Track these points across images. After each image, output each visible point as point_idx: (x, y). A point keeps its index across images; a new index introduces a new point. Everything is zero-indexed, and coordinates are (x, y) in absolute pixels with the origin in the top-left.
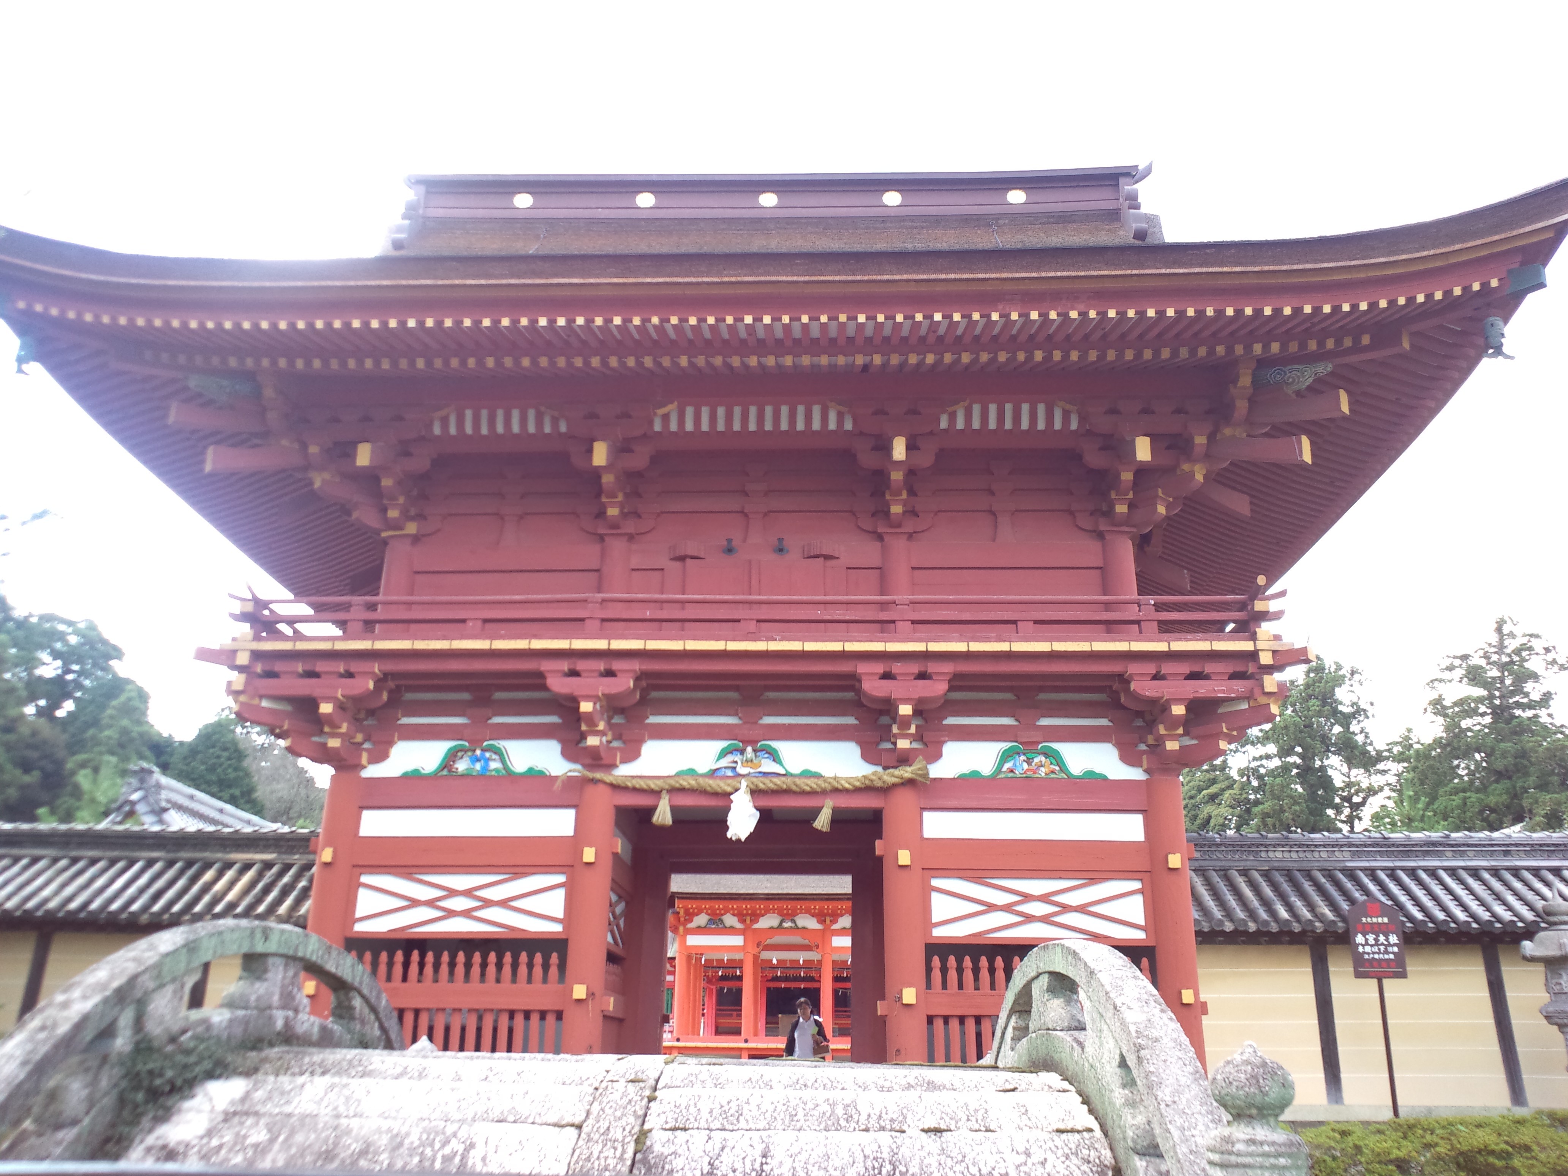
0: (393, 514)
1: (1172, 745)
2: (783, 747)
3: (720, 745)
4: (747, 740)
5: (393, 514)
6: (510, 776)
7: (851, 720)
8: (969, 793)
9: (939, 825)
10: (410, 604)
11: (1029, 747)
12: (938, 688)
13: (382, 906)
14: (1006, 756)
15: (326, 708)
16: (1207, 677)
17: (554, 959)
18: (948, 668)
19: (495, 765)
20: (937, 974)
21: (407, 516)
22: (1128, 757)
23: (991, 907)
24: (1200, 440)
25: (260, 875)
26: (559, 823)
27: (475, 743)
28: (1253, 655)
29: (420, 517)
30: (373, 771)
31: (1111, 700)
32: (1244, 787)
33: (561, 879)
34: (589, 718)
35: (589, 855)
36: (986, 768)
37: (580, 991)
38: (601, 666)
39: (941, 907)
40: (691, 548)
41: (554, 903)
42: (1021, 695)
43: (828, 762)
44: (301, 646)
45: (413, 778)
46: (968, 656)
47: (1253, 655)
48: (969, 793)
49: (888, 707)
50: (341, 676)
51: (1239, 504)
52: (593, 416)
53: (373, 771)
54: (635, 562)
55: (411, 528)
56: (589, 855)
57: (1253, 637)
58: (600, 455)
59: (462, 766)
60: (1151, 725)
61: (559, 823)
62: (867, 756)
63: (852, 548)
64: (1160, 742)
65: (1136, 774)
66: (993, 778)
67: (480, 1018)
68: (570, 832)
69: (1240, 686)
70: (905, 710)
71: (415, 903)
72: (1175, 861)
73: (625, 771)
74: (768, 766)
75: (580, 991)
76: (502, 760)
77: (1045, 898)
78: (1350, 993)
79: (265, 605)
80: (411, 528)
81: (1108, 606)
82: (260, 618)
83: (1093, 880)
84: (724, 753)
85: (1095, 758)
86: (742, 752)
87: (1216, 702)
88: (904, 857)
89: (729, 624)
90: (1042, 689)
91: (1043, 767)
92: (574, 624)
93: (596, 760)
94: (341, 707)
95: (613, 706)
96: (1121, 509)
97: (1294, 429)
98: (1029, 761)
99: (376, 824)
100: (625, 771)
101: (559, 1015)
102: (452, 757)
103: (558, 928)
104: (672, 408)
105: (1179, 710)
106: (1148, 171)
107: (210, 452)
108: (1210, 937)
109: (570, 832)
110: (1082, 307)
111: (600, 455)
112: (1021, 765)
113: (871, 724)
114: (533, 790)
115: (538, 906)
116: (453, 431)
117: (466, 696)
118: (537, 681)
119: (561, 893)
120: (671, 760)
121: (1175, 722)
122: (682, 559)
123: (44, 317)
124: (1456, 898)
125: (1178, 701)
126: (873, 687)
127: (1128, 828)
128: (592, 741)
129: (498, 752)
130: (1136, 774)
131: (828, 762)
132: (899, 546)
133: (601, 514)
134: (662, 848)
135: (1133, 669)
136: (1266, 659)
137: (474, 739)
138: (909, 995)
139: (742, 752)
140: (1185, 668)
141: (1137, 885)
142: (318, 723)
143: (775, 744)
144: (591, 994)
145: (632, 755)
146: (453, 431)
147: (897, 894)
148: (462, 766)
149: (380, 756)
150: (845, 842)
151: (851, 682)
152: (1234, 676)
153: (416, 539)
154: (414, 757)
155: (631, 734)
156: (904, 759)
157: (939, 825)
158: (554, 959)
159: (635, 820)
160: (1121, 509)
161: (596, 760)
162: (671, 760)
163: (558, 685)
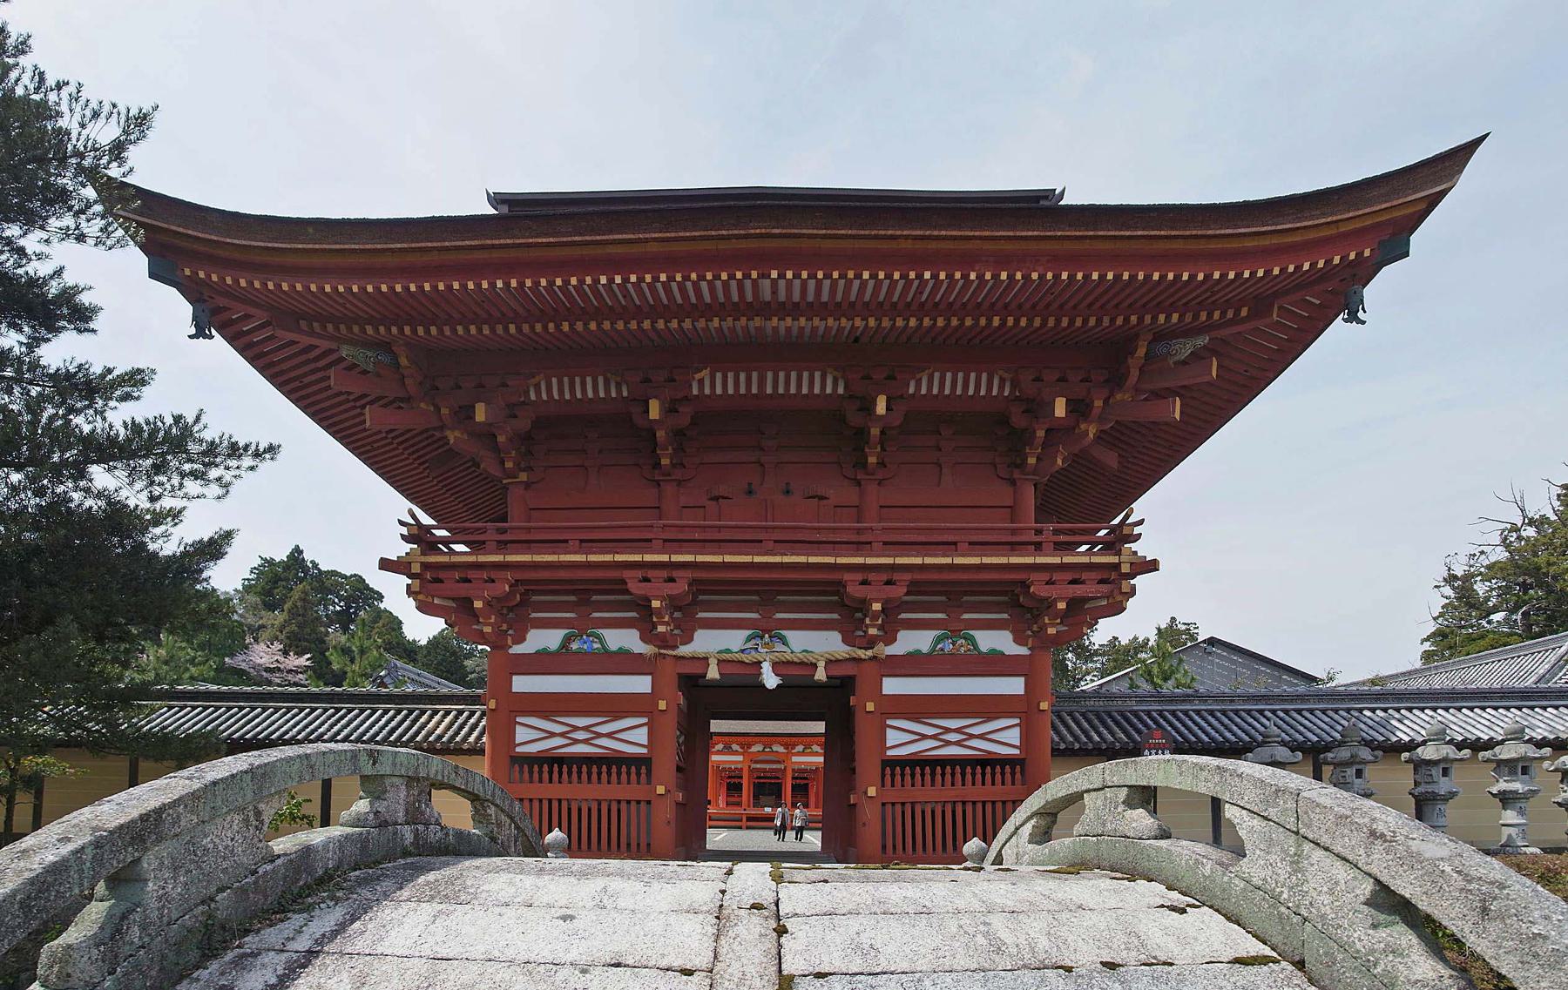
2: (790, 635)
6: (607, 653)
9: (893, 686)
10: (529, 529)
11: (955, 633)
14: (939, 640)
16: (1083, 582)
17: (643, 770)
20: (888, 778)
22: (1019, 640)
23: (924, 737)
25: (456, 718)
26: (641, 684)
29: (529, 469)
31: (1015, 601)
33: (645, 720)
34: (659, 612)
35: (662, 705)
36: (925, 649)
37: (661, 790)
38: (665, 574)
40: (722, 490)
41: (641, 736)
42: (953, 596)
43: (819, 646)
44: (455, 559)
45: (542, 654)
51: (1111, 459)
52: (647, 380)
53: (517, 649)
55: (523, 477)
56: (662, 705)
57: (1119, 553)
58: (654, 410)
59: (575, 646)
60: (1037, 617)
61: (641, 684)
63: (839, 492)
65: (1023, 651)
66: (929, 655)
70: (877, 606)
71: (552, 735)
72: (1044, 706)
73: (684, 650)
74: (779, 647)
75: (661, 790)
77: (958, 731)
80: (523, 477)
81: (1014, 531)
83: (989, 719)
84: (749, 639)
85: (997, 641)
88: (870, 707)
89: (754, 544)
90: (966, 593)
91: (963, 646)
92: (644, 544)
94: (488, 604)
95: (674, 604)
96: (1032, 461)
99: (521, 684)
100: (684, 650)
101: (649, 802)
102: (567, 640)
103: (645, 751)
104: (705, 373)
108: (1056, 752)
111: (654, 410)
112: (948, 646)
114: (623, 663)
115: (633, 737)
117: (573, 598)
118: (620, 586)
119: (645, 730)
122: (716, 499)
123: (207, 283)
124: (1201, 728)
125: (1062, 599)
127: (1014, 686)
128: (661, 629)
129: (598, 637)
130: (1023, 651)
131: (819, 646)
133: (657, 465)
134: (705, 699)
137: (581, 628)
138: (872, 791)
139: (762, 638)
140: (1069, 576)
142: (474, 615)
143: (784, 632)
144: (667, 791)
145: (689, 639)
147: (862, 727)
148: (575, 646)
149: (521, 639)
150: (831, 700)
151: (838, 587)
153: (527, 485)
156: (870, 643)
157: (893, 686)
158: (643, 770)
159: (692, 683)
160: (1032, 461)
161: (664, 642)
162: (715, 644)
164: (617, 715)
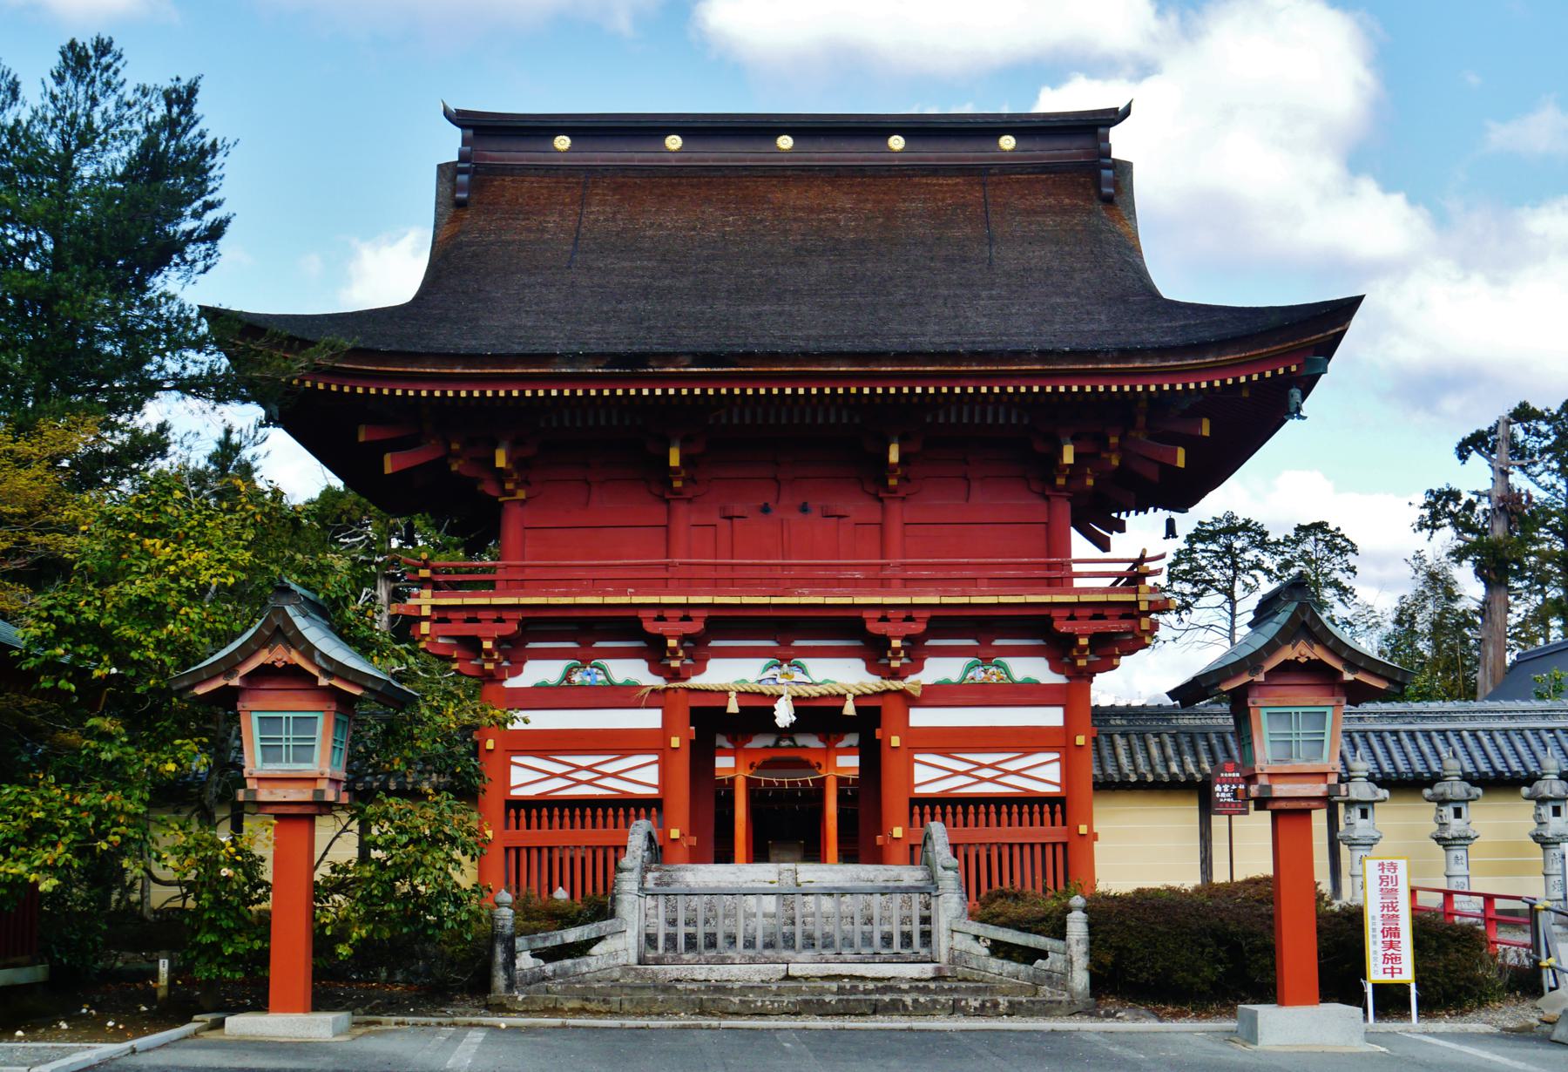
0: (509, 486)
1: (1082, 663)
4: (784, 657)
5: (509, 486)
6: (613, 687)
9: (920, 718)
11: (987, 660)
13: (528, 778)
14: (970, 668)
15: (488, 645)
18: (927, 614)
19: (601, 678)
21: (518, 486)
22: (1055, 668)
24: (1114, 440)
26: (651, 719)
27: (586, 661)
28: (1136, 603)
30: (511, 683)
32: (1470, 506)
33: (655, 758)
39: (921, 773)
41: (651, 775)
43: (842, 676)
46: (941, 605)
47: (1136, 603)
48: (939, 695)
49: (885, 641)
50: (496, 621)
54: (694, 519)
55: (521, 495)
61: (651, 719)
62: (872, 668)
63: (858, 508)
64: (1074, 660)
65: (1060, 679)
67: (594, 853)
68: (659, 725)
69: (1125, 625)
71: (553, 775)
72: (1080, 740)
73: (696, 681)
74: (799, 676)
75: (675, 834)
76: (606, 674)
78: (1219, 823)
80: (521, 495)
84: (767, 668)
86: (780, 666)
88: (895, 741)
97: (1178, 440)
98: (986, 671)
100: (696, 681)
103: (655, 791)
105: (1083, 641)
106: (1127, 112)
107: (387, 458)
109: (659, 725)
110: (1016, 383)
112: (979, 675)
113: (874, 652)
115: (641, 776)
119: (655, 768)
120: (730, 674)
122: (731, 518)
126: (873, 627)
130: (1060, 679)
131: (842, 676)
132: (895, 508)
135: (1055, 613)
136: (1144, 607)
138: (898, 832)
141: (1057, 756)
143: (802, 660)
144: (682, 835)
145: (700, 669)
149: (517, 671)
152: (1123, 617)
155: (698, 651)
157: (920, 718)
161: (674, 675)
162: (730, 674)
164: (625, 753)
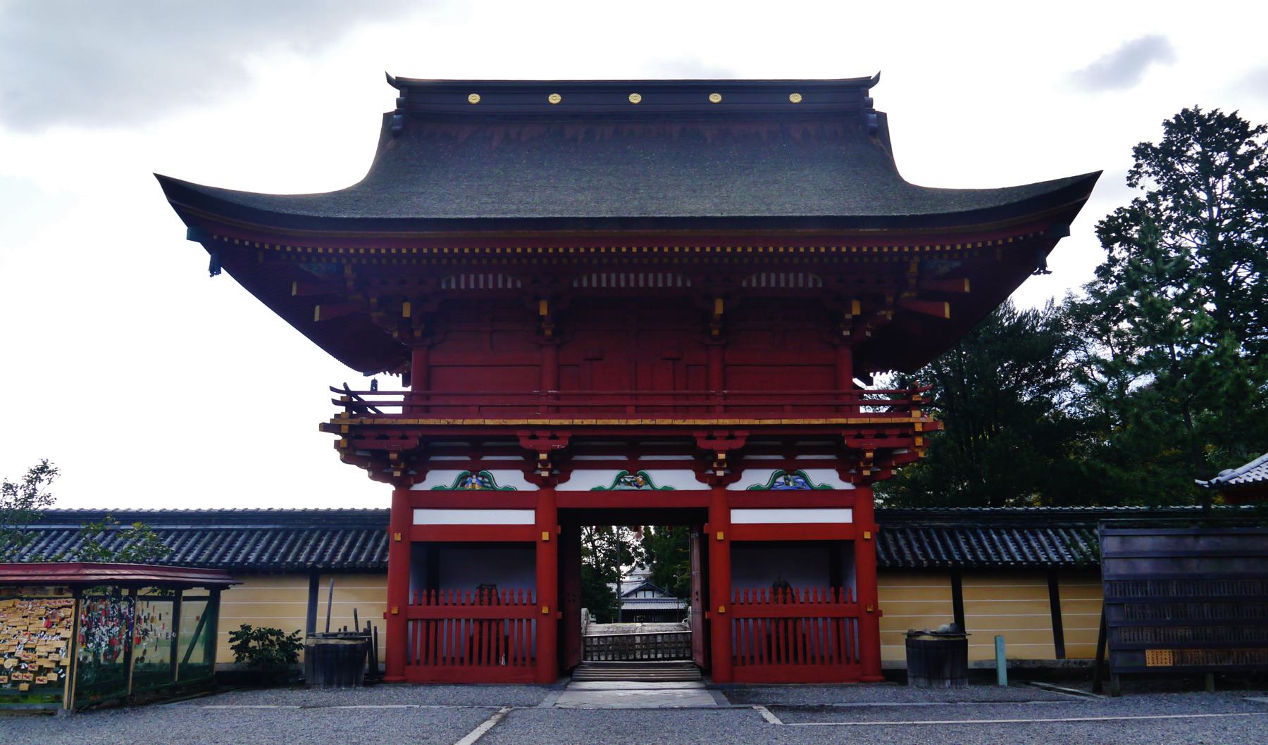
1: (867, 473)
3: (613, 474)
7: (689, 458)
8: (755, 499)
12: (739, 444)
18: (747, 433)
22: (843, 478)
30: (417, 487)
53: (417, 487)
64: (860, 470)
65: (848, 486)
68: (533, 522)
73: (561, 487)
79: (355, 394)
82: (349, 399)
87: (891, 450)
93: (547, 484)
100: (561, 487)
102: (462, 480)
109: (533, 522)
114: (510, 500)
116: (453, 286)
121: (868, 461)
126: (703, 444)
129: (488, 477)
130: (848, 486)
137: (476, 467)
145: (566, 479)
146: (453, 286)
149: (421, 479)
152: (900, 436)
154: (443, 479)
155: (563, 466)
163: (526, 443)
